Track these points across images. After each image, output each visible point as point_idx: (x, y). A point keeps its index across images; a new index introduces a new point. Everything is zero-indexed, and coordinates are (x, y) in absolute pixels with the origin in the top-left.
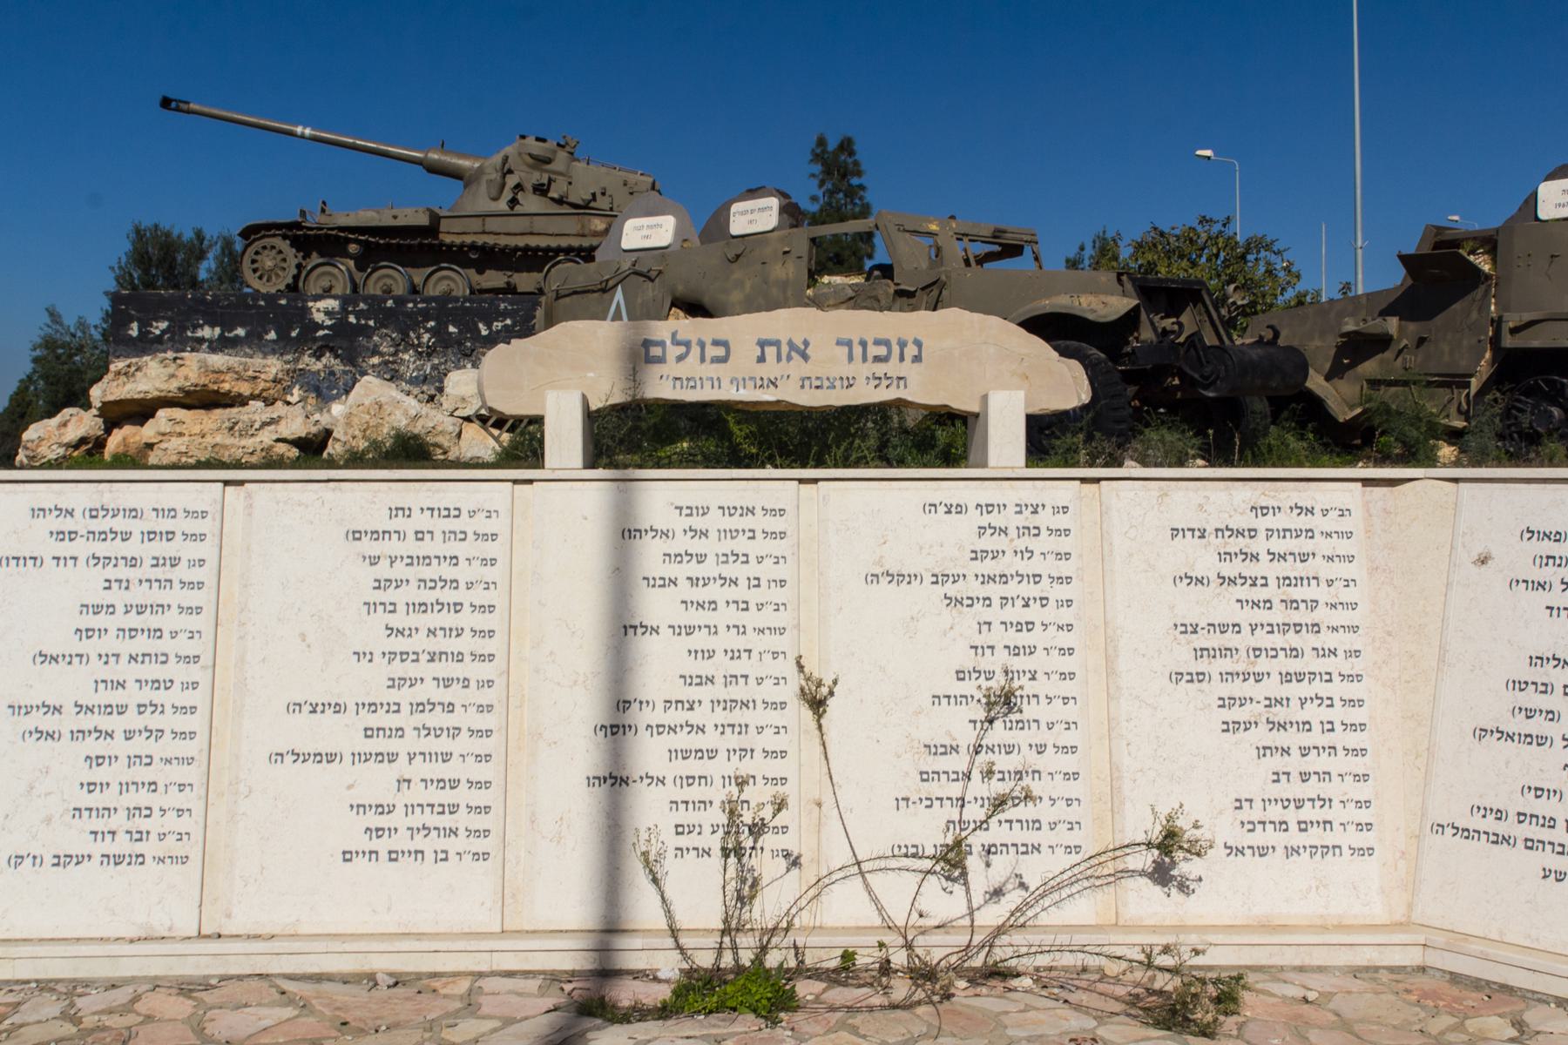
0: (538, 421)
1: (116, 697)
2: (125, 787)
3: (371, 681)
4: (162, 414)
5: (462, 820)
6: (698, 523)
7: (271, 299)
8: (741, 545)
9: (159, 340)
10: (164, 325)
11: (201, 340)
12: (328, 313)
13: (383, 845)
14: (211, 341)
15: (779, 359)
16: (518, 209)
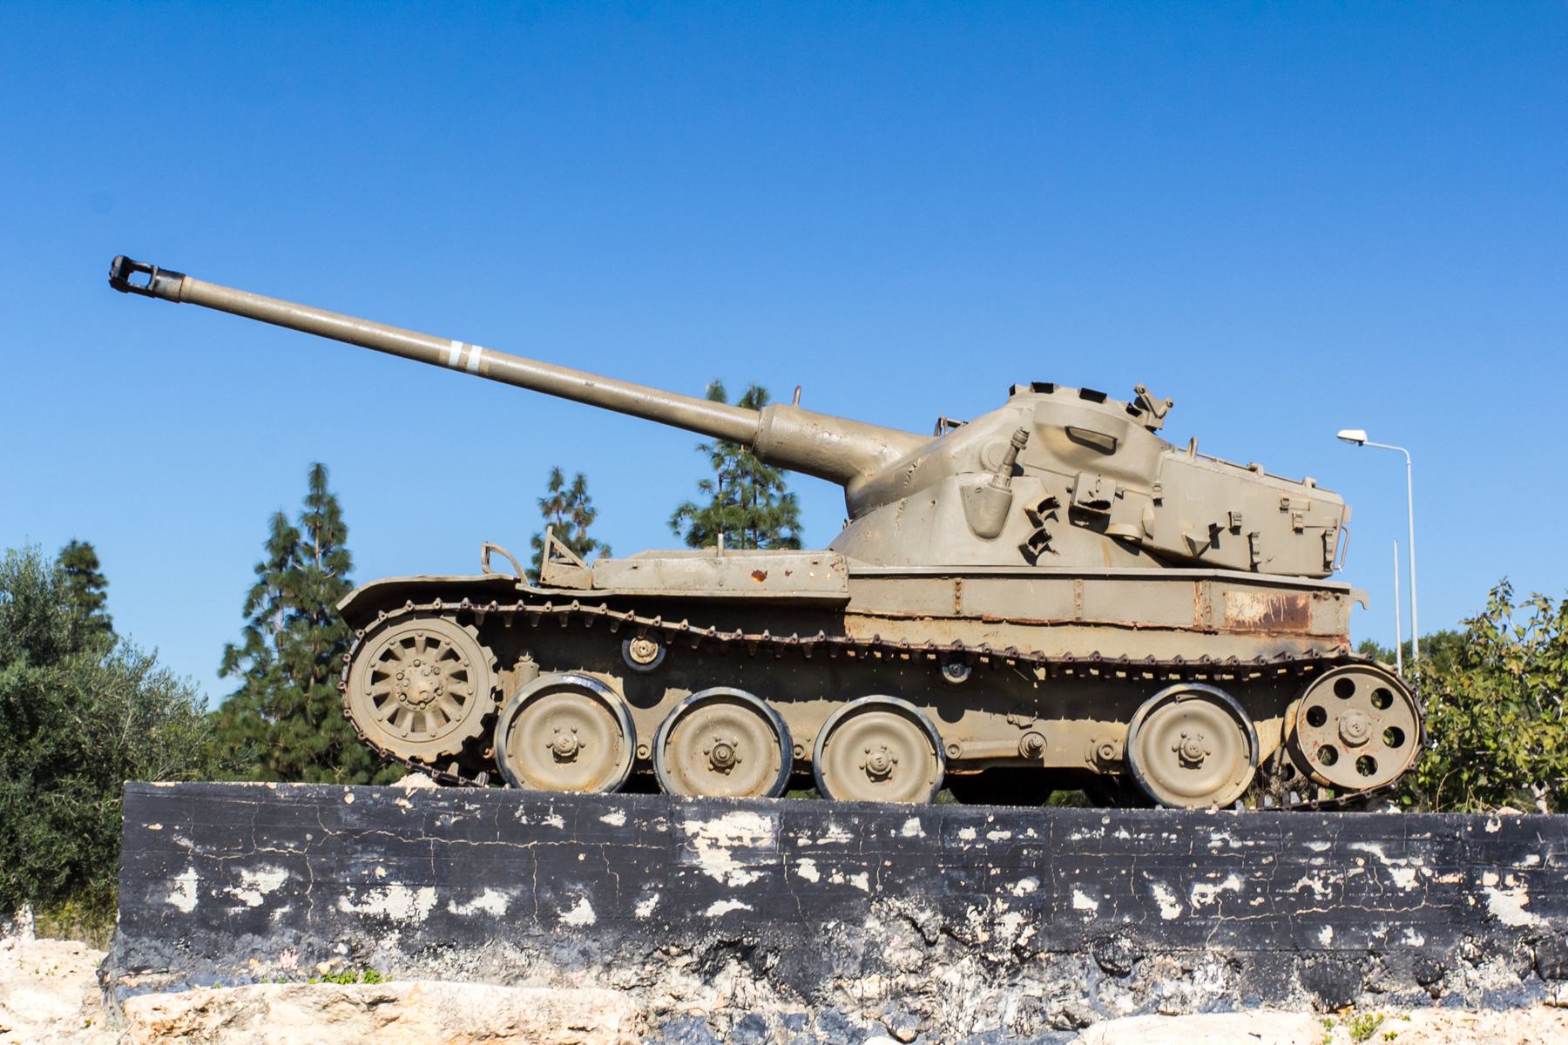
7: (581, 809)
9: (257, 922)
10: (273, 879)
11: (378, 925)
12: (739, 852)
14: (406, 928)
16: (1046, 562)
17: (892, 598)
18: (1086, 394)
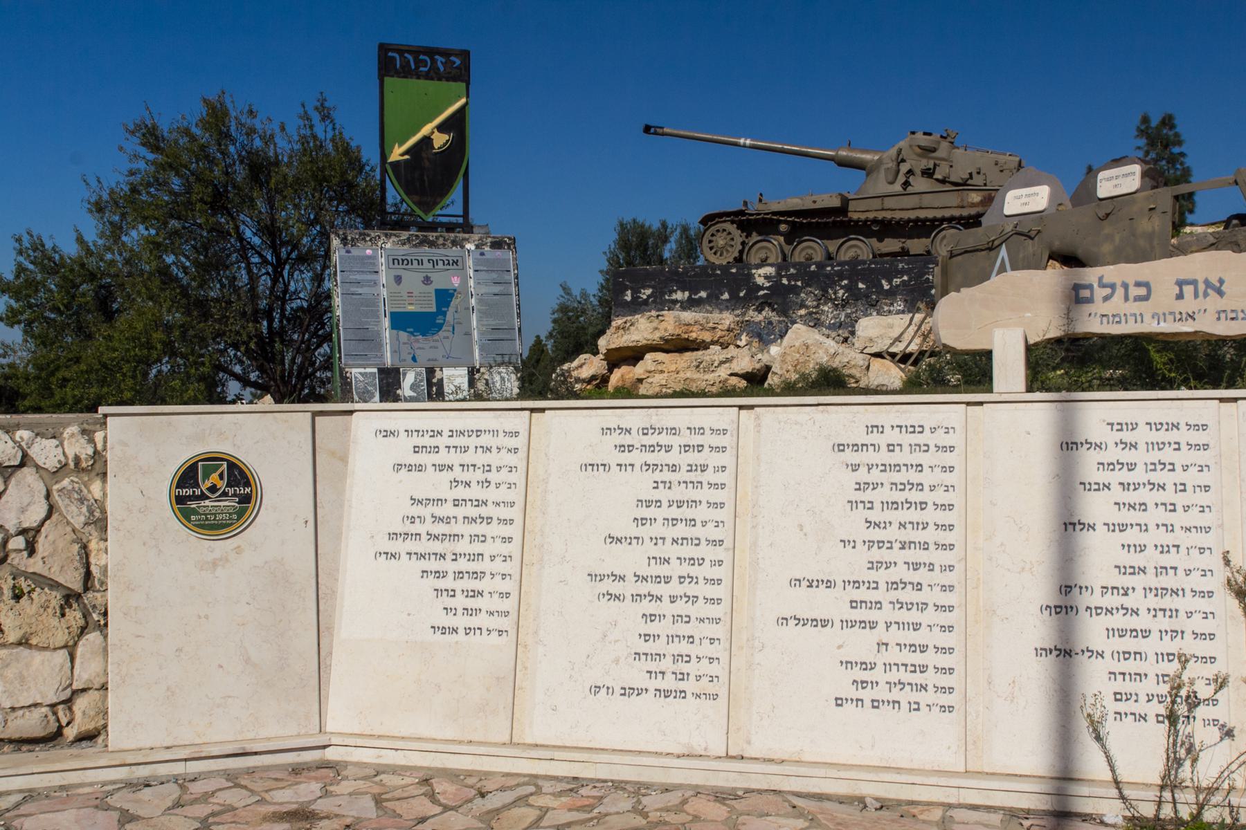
0: (988, 354)
1: (663, 570)
2: (671, 638)
3: (854, 563)
4: (648, 356)
5: (930, 678)
6: (1127, 436)
7: (725, 269)
8: (1168, 455)
9: (645, 302)
10: (649, 292)
11: (675, 302)
12: (767, 277)
13: (867, 695)
14: (682, 302)
15: (1196, 296)
16: (910, 189)
17: (862, 206)
18: (925, 134)
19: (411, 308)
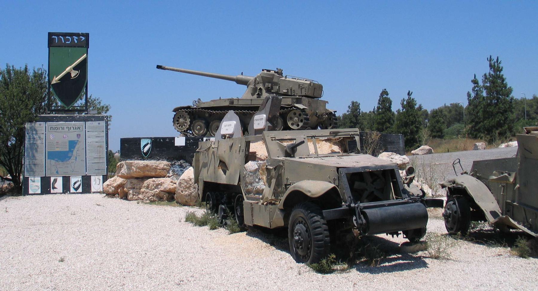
19: (57, 150)
